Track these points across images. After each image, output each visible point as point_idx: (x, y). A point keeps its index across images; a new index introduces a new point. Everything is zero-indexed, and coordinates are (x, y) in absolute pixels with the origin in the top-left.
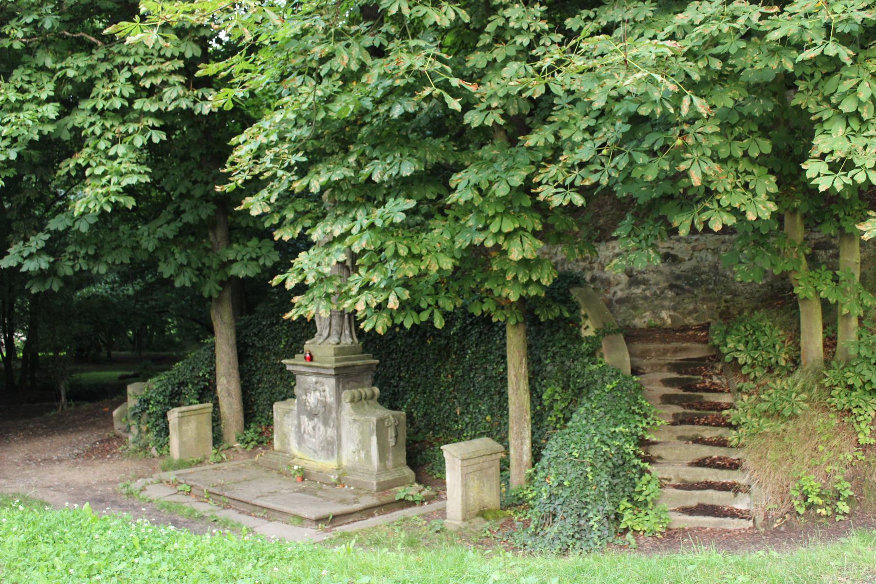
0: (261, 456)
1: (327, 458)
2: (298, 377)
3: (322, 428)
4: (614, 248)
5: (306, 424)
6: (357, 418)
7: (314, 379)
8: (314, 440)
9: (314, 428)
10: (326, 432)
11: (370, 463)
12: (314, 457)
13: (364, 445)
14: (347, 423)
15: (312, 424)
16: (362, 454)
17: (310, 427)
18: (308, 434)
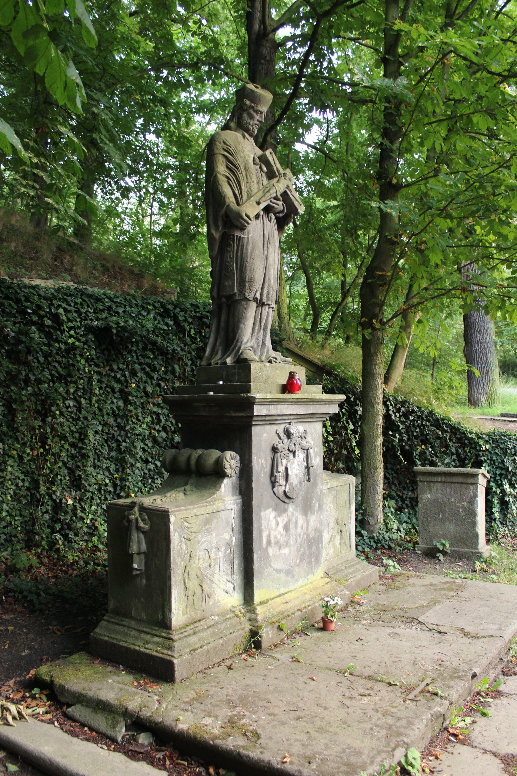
3: (301, 521)
5: (273, 523)
9: (286, 528)
15: (282, 520)
17: (281, 527)
18: (277, 543)
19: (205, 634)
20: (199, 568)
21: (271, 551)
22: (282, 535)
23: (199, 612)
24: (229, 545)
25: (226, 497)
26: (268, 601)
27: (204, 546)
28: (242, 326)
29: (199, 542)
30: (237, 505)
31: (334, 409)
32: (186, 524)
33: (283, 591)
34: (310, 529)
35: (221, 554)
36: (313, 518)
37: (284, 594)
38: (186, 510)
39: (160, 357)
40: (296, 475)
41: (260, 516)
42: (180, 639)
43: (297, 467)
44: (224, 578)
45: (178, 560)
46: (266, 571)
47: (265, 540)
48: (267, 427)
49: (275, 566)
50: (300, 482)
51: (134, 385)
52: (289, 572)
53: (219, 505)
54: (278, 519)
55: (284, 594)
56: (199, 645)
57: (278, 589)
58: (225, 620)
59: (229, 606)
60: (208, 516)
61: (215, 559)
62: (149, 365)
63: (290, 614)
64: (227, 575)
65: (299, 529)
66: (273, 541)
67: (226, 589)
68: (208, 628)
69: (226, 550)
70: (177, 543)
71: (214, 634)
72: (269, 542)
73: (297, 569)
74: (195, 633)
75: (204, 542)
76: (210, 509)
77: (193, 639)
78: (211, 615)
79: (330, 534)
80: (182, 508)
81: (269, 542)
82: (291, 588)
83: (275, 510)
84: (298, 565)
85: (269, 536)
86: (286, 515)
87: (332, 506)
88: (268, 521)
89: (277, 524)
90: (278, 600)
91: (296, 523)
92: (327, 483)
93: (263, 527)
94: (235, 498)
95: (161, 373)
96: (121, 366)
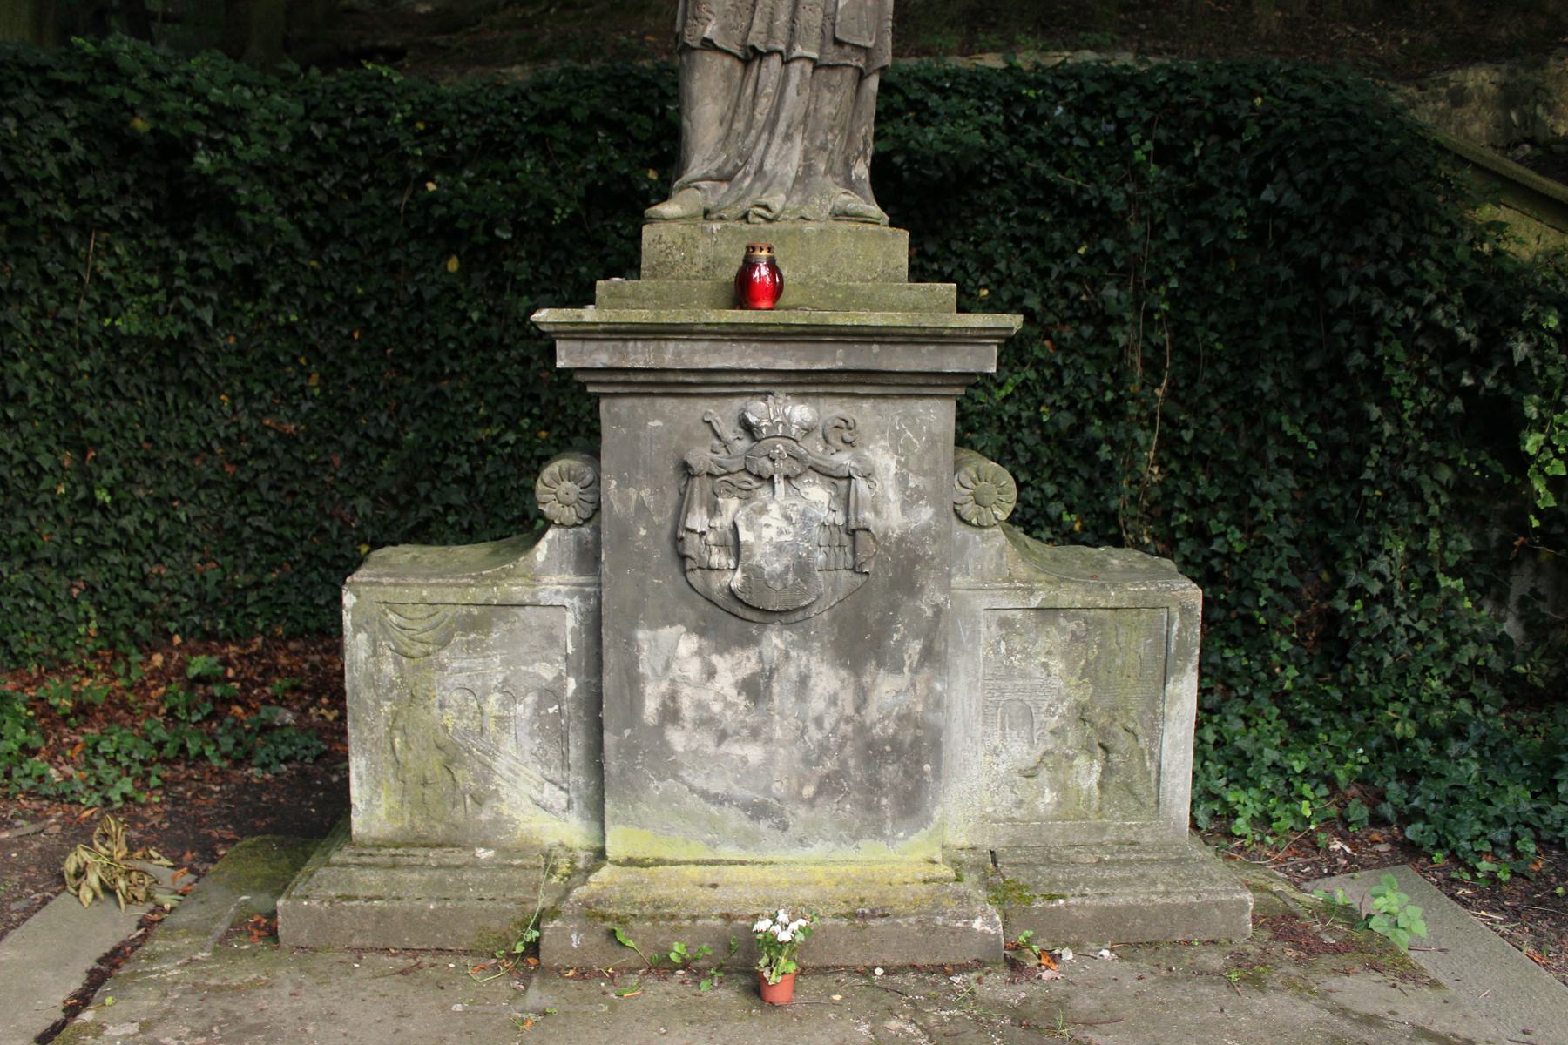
0: (318, 894)
1: (871, 825)
2: (615, 415)
3: (827, 680)
5: (693, 668)
6: (1068, 596)
7: (801, 412)
8: (754, 753)
9: (755, 688)
12: (747, 840)
13: (1106, 734)
14: (988, 631)
15: (731, 669)
16: (1087, 774)
17: (726, 682)
18: (706, 721)
19: (416, 876)
20: (445, 728)
21: (677, 739)
22: (729, 705)
23: (440, 828)
24: (551, 693)
25: (548, 574)
26: (659, 862)
27: (462, 678)
28: (686, 123)
29: (443, 668)
30: (585, 598)
31: (986, 361)
32: (392, 617)
33: (728, 852)
34: (872, 713)
35: (523, 709)
37: (730, 863)
38: (395, 585)
39: (1072, 221)
40: (780, 548)
41: (631, 641)
42: (345, 865)
43: (783, 524)
44: (535, 771)
45: (368, 696)
46: (656, 787)
47: (651, 707)
48: (668, 404)
49: (699, 783)
50: (803, 568)
51: (985, 292)
52: (758, 811)
53: (516, 589)
54: (715, 659)
55: (730, 863)
56: (371, 893)
57: (712, 844)
58: (503, 867)
59: (550, 840)
60: (475, 611)
61: (499, 719)
62: (1040, 241)
63: (684, 913)
64: (547, 764)
65: (817, 705)
66: (688, 712)
67: (537, 796)
68: (440, 867)
69: (539, 706)
70: (362, 655)
71: (441, 884)
72: (670, 713)
73: (802, 811)
74: (394, 866)
75: (461, 670)
76: (477, 594)
77: (373, 878)
78: (482, 845)
79: (1042, 748)
80: (385, 580)
81: (670, 713)
82: (775, 858)
83: (702, 632)
84: (811, 803)
85: (673, 696)
86: (752, 653)
87: (1057, 665)
89: (711, 673)
90: (693, 872)
91: (803, 681)
92: (1031, 591)
93: (644, 669)
94: (582, 579)
95: (1074, 262)
96: (956, 245)
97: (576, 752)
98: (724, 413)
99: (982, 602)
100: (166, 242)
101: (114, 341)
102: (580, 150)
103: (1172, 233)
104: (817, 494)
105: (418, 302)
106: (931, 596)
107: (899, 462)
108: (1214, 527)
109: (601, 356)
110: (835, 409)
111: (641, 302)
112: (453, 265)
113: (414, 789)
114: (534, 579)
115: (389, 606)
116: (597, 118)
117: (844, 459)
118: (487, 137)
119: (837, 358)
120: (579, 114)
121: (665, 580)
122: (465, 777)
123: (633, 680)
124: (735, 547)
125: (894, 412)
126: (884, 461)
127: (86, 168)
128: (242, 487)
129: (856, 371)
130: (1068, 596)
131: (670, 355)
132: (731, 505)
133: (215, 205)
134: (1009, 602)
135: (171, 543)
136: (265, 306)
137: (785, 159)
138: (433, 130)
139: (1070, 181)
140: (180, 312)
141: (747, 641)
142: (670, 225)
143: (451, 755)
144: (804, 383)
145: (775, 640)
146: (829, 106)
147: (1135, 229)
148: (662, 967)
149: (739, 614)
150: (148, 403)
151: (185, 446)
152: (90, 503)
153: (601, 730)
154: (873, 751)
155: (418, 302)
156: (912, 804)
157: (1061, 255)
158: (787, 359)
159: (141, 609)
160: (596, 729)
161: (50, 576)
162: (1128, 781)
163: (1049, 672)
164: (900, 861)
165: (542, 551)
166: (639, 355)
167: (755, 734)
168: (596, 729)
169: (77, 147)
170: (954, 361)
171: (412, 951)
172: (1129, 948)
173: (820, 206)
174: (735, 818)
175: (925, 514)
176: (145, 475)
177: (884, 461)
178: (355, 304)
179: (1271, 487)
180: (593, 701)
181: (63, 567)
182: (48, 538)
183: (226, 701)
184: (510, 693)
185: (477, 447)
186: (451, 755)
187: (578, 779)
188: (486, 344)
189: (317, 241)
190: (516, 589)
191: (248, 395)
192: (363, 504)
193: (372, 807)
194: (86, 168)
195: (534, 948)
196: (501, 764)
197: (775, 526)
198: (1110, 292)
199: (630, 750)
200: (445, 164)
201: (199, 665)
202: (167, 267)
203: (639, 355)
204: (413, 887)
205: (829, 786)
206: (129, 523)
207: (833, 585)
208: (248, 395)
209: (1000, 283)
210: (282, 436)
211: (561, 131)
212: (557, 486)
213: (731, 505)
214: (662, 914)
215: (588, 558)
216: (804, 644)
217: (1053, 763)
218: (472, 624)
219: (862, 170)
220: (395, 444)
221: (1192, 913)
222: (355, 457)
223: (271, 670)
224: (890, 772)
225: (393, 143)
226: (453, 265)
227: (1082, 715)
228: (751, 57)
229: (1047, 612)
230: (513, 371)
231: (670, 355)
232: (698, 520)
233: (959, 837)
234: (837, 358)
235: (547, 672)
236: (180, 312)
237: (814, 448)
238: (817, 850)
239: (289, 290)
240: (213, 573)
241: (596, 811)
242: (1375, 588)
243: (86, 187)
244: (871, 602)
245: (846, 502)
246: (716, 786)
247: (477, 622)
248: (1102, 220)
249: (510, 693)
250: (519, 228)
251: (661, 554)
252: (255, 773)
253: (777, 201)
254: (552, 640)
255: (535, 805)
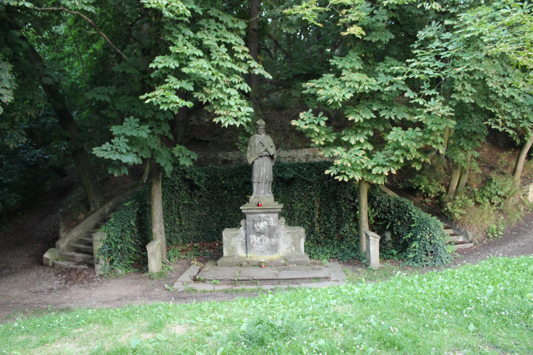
1: (272, 253)
4: (305, 152)
5: (255, 239)
6: (290, 231)
7: (264, 215)
8: (261, 246)
9: (261, 240)
10: (271, 241)
11: (300, 251)
12: (261, 255)
13: (295, 244)
14: (283, 235)
15: (259, 239)
16: (294, 248)
18: (257, 244)
21: (254, 245)
24: (242, 242)
25: (242, 230)
35: (240, 243)
36: (273, 240)
47: (251, 242)
50: (265, 229)
52: (262, 252)
53: (239, 232)
72: (253, 243)
81: (253, 243)
83: (256, 235)
88: (254, 238)
91: (265, 240)
97: (245, 247)
98: (257, 216)
99: (282, 232)
100: (190, 191)
101: (184, 204)
102: (242, 177)
103: (319, 185)
104: (266, 222)
105: (222, 197)
106: (277, 231)
107: (273, 219)
108: (326, 223)
109: (246, 211)
110: (267, 215)
111: (249, 206)
112: (226, 192)
113: (230, 251)
114: (240, 231)
115: (227, 234)
116: (244, 173)
117: (268, 219)
118: (230, 176)
119: (266, 211)
120: (242, 173)
121: (252, 231)
122: (234, 250)
123: (250, 240)
124: (259, 228)
125: (272, 215)
126: (272, 219)
127: (181, 183)
128: (199, 222)
129: (269, 211)
130: (290, 231)
131: (252, 211)
132: (258, 224)
133: (198, 188)
134: (285, 232)
135: (190, 230)
136: (203, 199)
137: (262, 192)
138: (223, 175)
139: (306, 179)
140: (193, 200)
141: (260, 236)
142: (252, 198)
143: (233, 248)
144: (264, 213)
145: (263, 236)
146: (266, 186)
147: (314, 185)
148: (253, 266)
149: (259, 234)
150: (188, 212)
151: (192, 217)
152: (181, 225)
153: (247, 245)
154: (272, 246)
155: (222, 197)
156: (276, 251)
157: (306, 188)
158: (262, 211)
159: (187, 238)
160: (246, 245)
161: (176, 234)
162: (298, 249)
163: (289, 239)
164: (275, 257)
165: (241, 228)
166: (249, 211)
167: (261, 245)
168: (246, 245)
169: (180, 181)
170: (277, 210)
171: (230, 265)
172: (297, 264)
173: (266, 196)
174: (260, 253)
175: (276, 224)
176: (187, 221)
177: (272, 219)
178: (213, 198)
179: (333, 218)
180: (246, 242)
181: (178, 233)
182: (177, 229)
183: (199, 249)
184: (238, 242)
185: (235, 220)
186: (233, 248)
187: (245, 250)
188: (231, 202)
189: (208, 190)
190: (239, 232)
191: (200, 210)
192: (215, 224)
193: (225, 253)
194: (181, 183)
195: (241, 265)
196: (238, 249)
197: (262, 225)
198: (312, 193)
199: (250, 247)
200: (225, 179)
201: (195, 245)
202: (190, 195)
203: (249, 211)
204: (230, 260)
205: (268, 250)
206: (186, 227)
207: (267, 231)
208: (200, 210)
209: (298, 192)
210: (204, 215)
211: (239, 175)
212: (242, 222)
213: (258, 224)
214: (253, 261)
215: (245, 229)
216: (265, 236)
217: (291, 247)
218: (235, 235)
219: (270, 191)
220: (219, 216)
221: (303, 261)
222: (213, 218)
223: (204, 246)
224: (274, 248)
225: (218, 177)
226: (226, 192)
227: (292, 243)
228: (259, 183)
229: (288, 233)
230: (234, 206)
231: (252, 211)
232: (255, 225)
233: (281, 255)
234: (266, 211)
235: (242, 240)
236: (193, 200)
237: (265, 218)
238: (267, 256)
239: (205, 197)
240: (196, 234)
241: (247, 253)
242: (345, 231)
243: (181, 185)
244: (271, 232)
245: (268, 223)
246: (258, 250)
247: (235, 235)
248: (311, 184)
249: (238, 242)
250: (234, 187)
251: (252, 228)
252: (206, 257)
253: (261, 196)
254: (242, 237)
255: (241, 252)
